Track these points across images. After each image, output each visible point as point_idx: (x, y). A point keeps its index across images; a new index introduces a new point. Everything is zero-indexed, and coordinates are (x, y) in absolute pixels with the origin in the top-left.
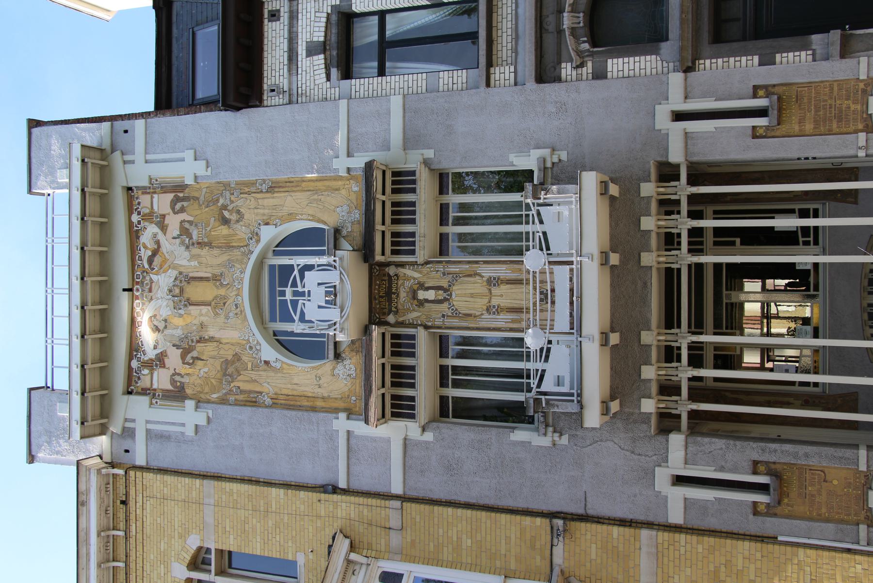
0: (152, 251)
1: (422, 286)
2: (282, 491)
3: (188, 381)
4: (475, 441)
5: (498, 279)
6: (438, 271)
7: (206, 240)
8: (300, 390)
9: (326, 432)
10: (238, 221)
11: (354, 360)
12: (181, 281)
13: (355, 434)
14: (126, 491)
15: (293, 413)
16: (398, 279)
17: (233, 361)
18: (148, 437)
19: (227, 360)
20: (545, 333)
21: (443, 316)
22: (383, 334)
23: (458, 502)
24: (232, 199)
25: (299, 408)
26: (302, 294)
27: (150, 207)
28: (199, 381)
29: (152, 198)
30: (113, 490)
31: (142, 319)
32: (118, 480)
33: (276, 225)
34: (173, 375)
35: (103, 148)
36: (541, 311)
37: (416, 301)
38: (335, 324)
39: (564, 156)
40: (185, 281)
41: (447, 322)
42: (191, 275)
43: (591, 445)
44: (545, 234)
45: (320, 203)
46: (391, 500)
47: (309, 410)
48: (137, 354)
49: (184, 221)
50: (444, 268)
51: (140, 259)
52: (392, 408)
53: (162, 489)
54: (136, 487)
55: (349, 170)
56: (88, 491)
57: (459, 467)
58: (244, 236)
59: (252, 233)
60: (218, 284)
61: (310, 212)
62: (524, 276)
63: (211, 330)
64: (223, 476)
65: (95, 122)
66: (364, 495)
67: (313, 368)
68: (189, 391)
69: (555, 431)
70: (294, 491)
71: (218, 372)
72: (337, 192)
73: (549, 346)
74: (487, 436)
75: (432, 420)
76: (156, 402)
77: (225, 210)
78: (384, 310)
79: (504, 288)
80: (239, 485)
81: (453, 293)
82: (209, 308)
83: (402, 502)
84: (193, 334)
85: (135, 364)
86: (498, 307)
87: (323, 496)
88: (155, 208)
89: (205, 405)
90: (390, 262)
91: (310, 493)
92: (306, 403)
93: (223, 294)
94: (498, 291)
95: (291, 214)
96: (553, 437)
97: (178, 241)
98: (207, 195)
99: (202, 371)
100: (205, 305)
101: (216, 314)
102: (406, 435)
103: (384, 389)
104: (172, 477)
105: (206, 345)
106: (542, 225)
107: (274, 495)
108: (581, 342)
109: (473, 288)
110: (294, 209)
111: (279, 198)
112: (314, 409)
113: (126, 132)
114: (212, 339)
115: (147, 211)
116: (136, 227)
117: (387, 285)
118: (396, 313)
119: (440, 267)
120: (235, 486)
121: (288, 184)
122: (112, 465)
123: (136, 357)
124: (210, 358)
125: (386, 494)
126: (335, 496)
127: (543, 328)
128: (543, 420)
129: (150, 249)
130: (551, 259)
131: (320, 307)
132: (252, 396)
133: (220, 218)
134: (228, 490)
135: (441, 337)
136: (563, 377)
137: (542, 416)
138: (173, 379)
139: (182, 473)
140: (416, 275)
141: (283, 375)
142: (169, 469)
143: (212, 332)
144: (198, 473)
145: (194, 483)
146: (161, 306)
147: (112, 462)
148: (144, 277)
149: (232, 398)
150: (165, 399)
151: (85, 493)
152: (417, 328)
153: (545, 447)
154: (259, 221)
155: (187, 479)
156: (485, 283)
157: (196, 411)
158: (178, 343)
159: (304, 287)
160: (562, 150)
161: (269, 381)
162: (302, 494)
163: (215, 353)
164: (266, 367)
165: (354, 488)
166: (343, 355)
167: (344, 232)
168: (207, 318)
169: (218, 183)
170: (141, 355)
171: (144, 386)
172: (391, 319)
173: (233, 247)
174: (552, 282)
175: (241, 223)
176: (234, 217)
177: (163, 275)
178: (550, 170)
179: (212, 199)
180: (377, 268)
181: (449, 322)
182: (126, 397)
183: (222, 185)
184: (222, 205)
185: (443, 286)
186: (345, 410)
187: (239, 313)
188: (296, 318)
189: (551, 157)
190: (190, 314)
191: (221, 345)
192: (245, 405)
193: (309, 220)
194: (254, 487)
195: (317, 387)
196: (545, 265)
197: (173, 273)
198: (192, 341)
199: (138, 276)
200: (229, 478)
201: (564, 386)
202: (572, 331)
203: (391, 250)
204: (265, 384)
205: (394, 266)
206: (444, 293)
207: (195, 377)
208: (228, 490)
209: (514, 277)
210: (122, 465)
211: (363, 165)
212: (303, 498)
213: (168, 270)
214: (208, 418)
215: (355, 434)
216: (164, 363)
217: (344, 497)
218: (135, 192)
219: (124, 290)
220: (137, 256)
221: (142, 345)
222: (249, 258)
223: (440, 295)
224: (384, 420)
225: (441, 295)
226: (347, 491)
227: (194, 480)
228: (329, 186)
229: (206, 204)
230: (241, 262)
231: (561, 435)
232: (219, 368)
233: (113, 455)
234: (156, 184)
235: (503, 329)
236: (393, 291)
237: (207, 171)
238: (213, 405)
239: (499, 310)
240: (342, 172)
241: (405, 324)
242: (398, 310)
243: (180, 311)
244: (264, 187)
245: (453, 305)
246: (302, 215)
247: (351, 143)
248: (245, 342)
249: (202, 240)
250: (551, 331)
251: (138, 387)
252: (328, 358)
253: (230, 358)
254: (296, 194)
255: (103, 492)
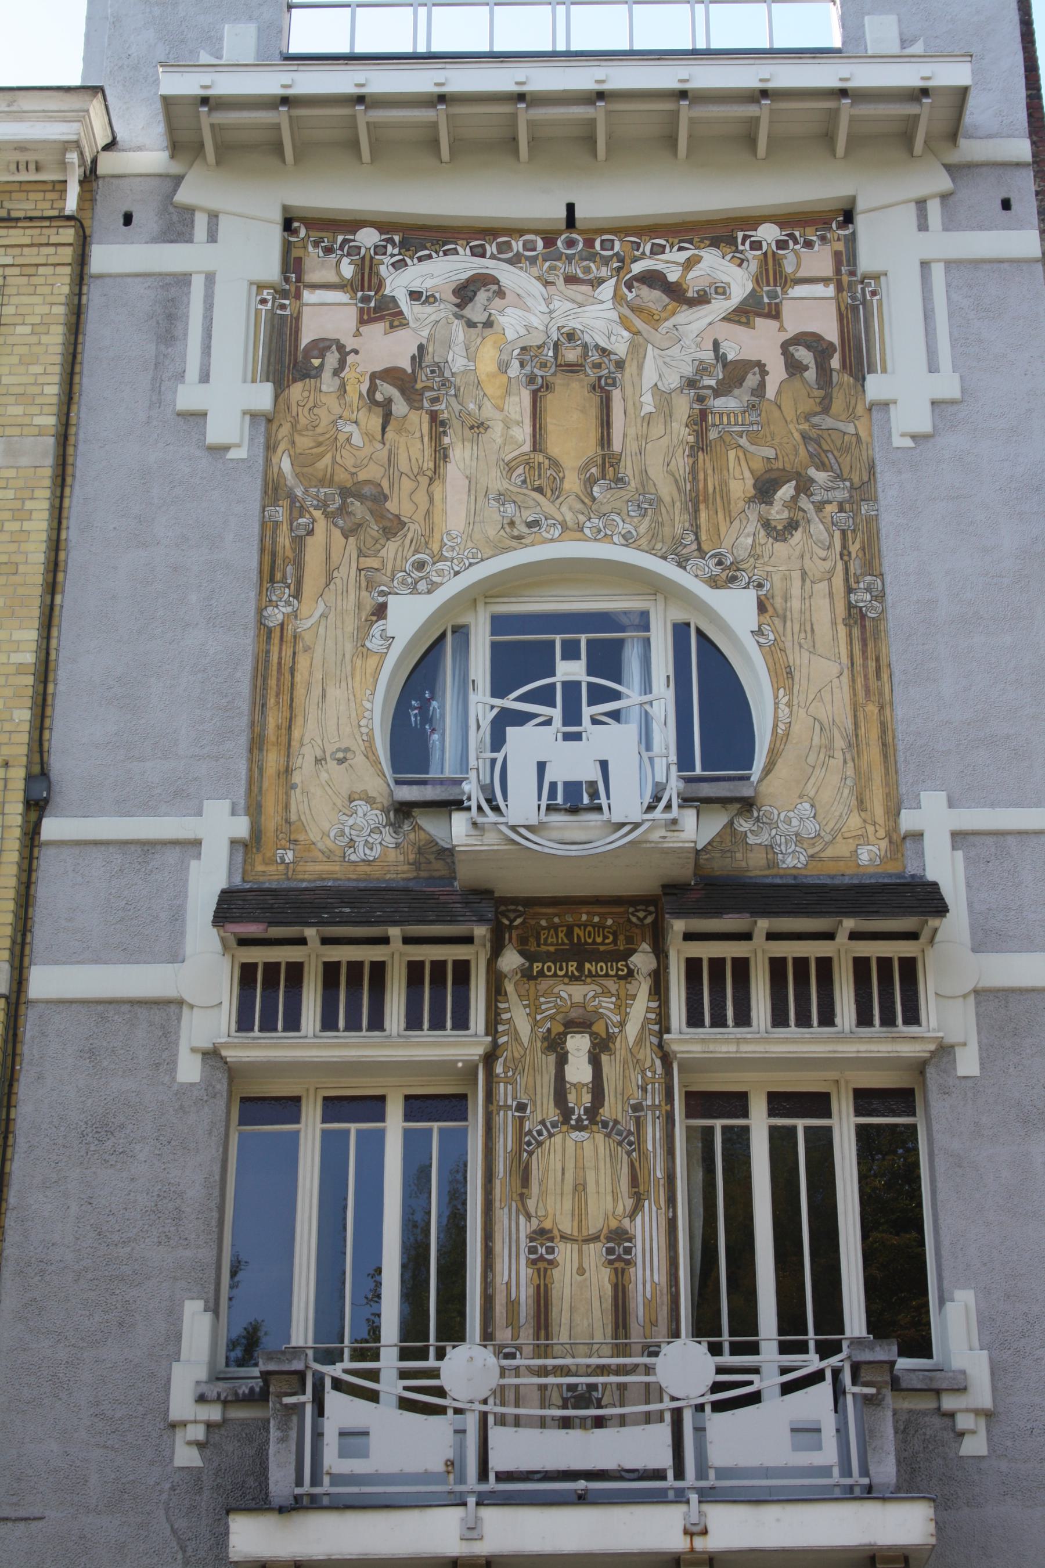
0: (677, 284)
1: (601, 1047)
2: (29, 658)
3: (324, 388)
4: (178, 1201)
5: (628, 1262)
6: (644, 1090)
7: (713, 435)
8: (308, 702)
9: (195, 779)
10: (767, 524)
11: (392, 856)
12: (597, 366)
13: (194, 864)
14: (18, 219)
15: (245, 688)
16: (620, 978)
17: (382, 517)
18: (168, 280)
19: (386, 498)
20: (485, 1402)
21: (521, 1107)
22: (468, 940)
23: (9, 1155)
24: (829, 508)
25: (259, 705)
26: (572, 716)
27: (801, 274)
28: (324, 423)
29: (825, 281)
30: (21, 182)
31: (493, 257)
32: (50, 196)
33: (759, 632)
34: (341, 348)
35: (962, 142)
36: (543, 1388)
37: (561, 1029)
38: (496, 809)
39: (975, 1446)
40: (600, 378)
41: (506, 1116)
42: (616, 394)
43: (174, 1531)
44: (755, 1398)
45: (822, 756)
46: (12, 966)
47: (253, 732)
48: (394, 245)
49: (764, 373)
50: (653, 1107)
51: (657, 250)
52: (266, 965)
53: (29, 320)
54: (32, 245)
55: (918, 836)
56: (19, 116)
57: (106, 1157)
58: (727, 543)
59: (736, 566)
60: (594, 470)
61: (796, 728)
62: (636, 1337)
63: (467, 454)
64: (67, 491)
65: (1030, 115)
66: (23, 887)
67: (370, 742)
68: (297, 391)
69: (209, 1426)
70: (30, 692)
71: (353, 474)
72: (854, 802)
73: (450, 1412)
74: (193, 1236)
75: (233, 1072)
76: (264, 301)
77: (798, 490)
78: (531, 940)
79: (602, 1278)
80: (44, 536)
81: (585, 1135)
82: (527, 447)
83: (6, 997)
84: (452, 400)
85: (368, 238)
86: (551, 1262)
87: (18, 774)
88: (799, 291)
89: (262, 440)
90: (667, 957)
91: (25, 738)
92: (271, 722)
93: (567, 485)
94: (593, 1264)
95: (790, 674)
96: (196, 1422)
97: (708, 355)
98: (835, 435)
99: (350, 428)
100: (534, 436)
101: (510, 468)
102: (192, 1007)
103: (318, 941)
104: (59, 349)
105: (426, 439)
106: (777, 1390)
107: (18, 635)
108: (465, 1504)
109: (602, 1190)
110: (804, 682)
111: (835, 638)
112: (257, 744)
113: (1006, 205)
114: (441, 454)
115: (789, 267)
116: (745, 238)
117: (602, 948)
118: (527, 975)
119: (653, 1098)
120: (39, 525)
121: (871, 665)
122: (90, 177)
123: (387, 240)
124: (390, 451)
125: (27, 951)
126: (20, 808)
127: (500, 1393)
128: (240, 1392)
129: (684, 276)
130: (688, 1416)
131: (541, 766)
132: (289, 569)
133: (773, 475)
134: (29, 505)
135: (463, 1097)
136: (363, 1453)
137: (252, 1389)
138: (330, 347)
139: (72, 374)
140: (632, 1030)
141: (348, 657)
142: (80, 337)
143: (460, 454)
144: (73, 420)
145: (46, 409)
146: (528, 310)
147: (97, 177)
148: (606, 261)
149: (280, 513)
150: (273, 326)
151: (14, 108)
152: (487, 1034)
153: (166, 1401)
154: (768, 586)
155: (54, 389)
156: (614, 1224)
157: (244, 413)
158: (428, 359)
159: (595, 721)
160: (990, 1439)
161: (332, 616)
162: (23, 715)
163: (404, 466)
164: (369, 604)
165: (41, 862)
166: (406, 827)
167: (744, 825)
168: (499, 441)
169: (872, 468)
170: (392, 255)
171: (308, 264)
172: (511, 960)
173: (697, 511)
174: (623, 1421)
175: (763, 533)
176: (777, 513)
177: (614, 315)
178: (932, 1405)
179: (825, 452)
180: (649, 920)
181: (506, 1121)
182: (278, 217)
183: (865, 479)
184: (812, 481)
185: (602, 1105)
186: (256, 832)
187: (516, 533)
188: (509, 703)
189: (967, 1410)
190: (508, 392)
191: (426, 480)
192: (262, 550)
193: (775, 726)
194: (39, 580)
195: (319, 753)
196: (673, 1399)
197: (620, 344)
198: (435, 400)
199: (608, 245)
200: (61, 508)
201: (343, 1454)
202: (492, 1476)
203: (700, 960)
204: (321, 608)
205: (654, 965)
206: (586, 1110)
207: (337, 410)
208: (29, 505)
209: (632, 1305)
210: (87, 205)
211: (931, 876)
212: (12, 720)
213: (627, 329)
214: (226, 448)
215: (194, 864)
216: (371, 321)
217: (17, 832)
218: (841, 232)
219: (571, 208)
220: (662, 242)
221: (420, 259)
222: (665, 558)
223: (579, 1096)
224: (233, 942)
225: (580, 1101)
226: (32, 839)
227: (54, 409)
228: (870, 779)
229: (813, 433)
230: (654, 535)
231: (201, 1445)
232: (362, 476)
233: (115, 181)
234: (863, 290)
235: (490, 1275)
236: (587, 965)
237: (903, 435)
238: (261, 461)
239: (541, 1265)
240: (908, 821)
241: (497, 1001)
242: (535, 978)
243: (515, 364)
244: (861, 598)
245: (551, 1135)
246: (789, 704)
247: (990, 840)
248: (436, 547)
249: (714, 425)
250: (491, 1419)
251: (305, 247)
252: (398, 782)
253: (391, 506)
254: (846, 688)
255: (22, 157)
